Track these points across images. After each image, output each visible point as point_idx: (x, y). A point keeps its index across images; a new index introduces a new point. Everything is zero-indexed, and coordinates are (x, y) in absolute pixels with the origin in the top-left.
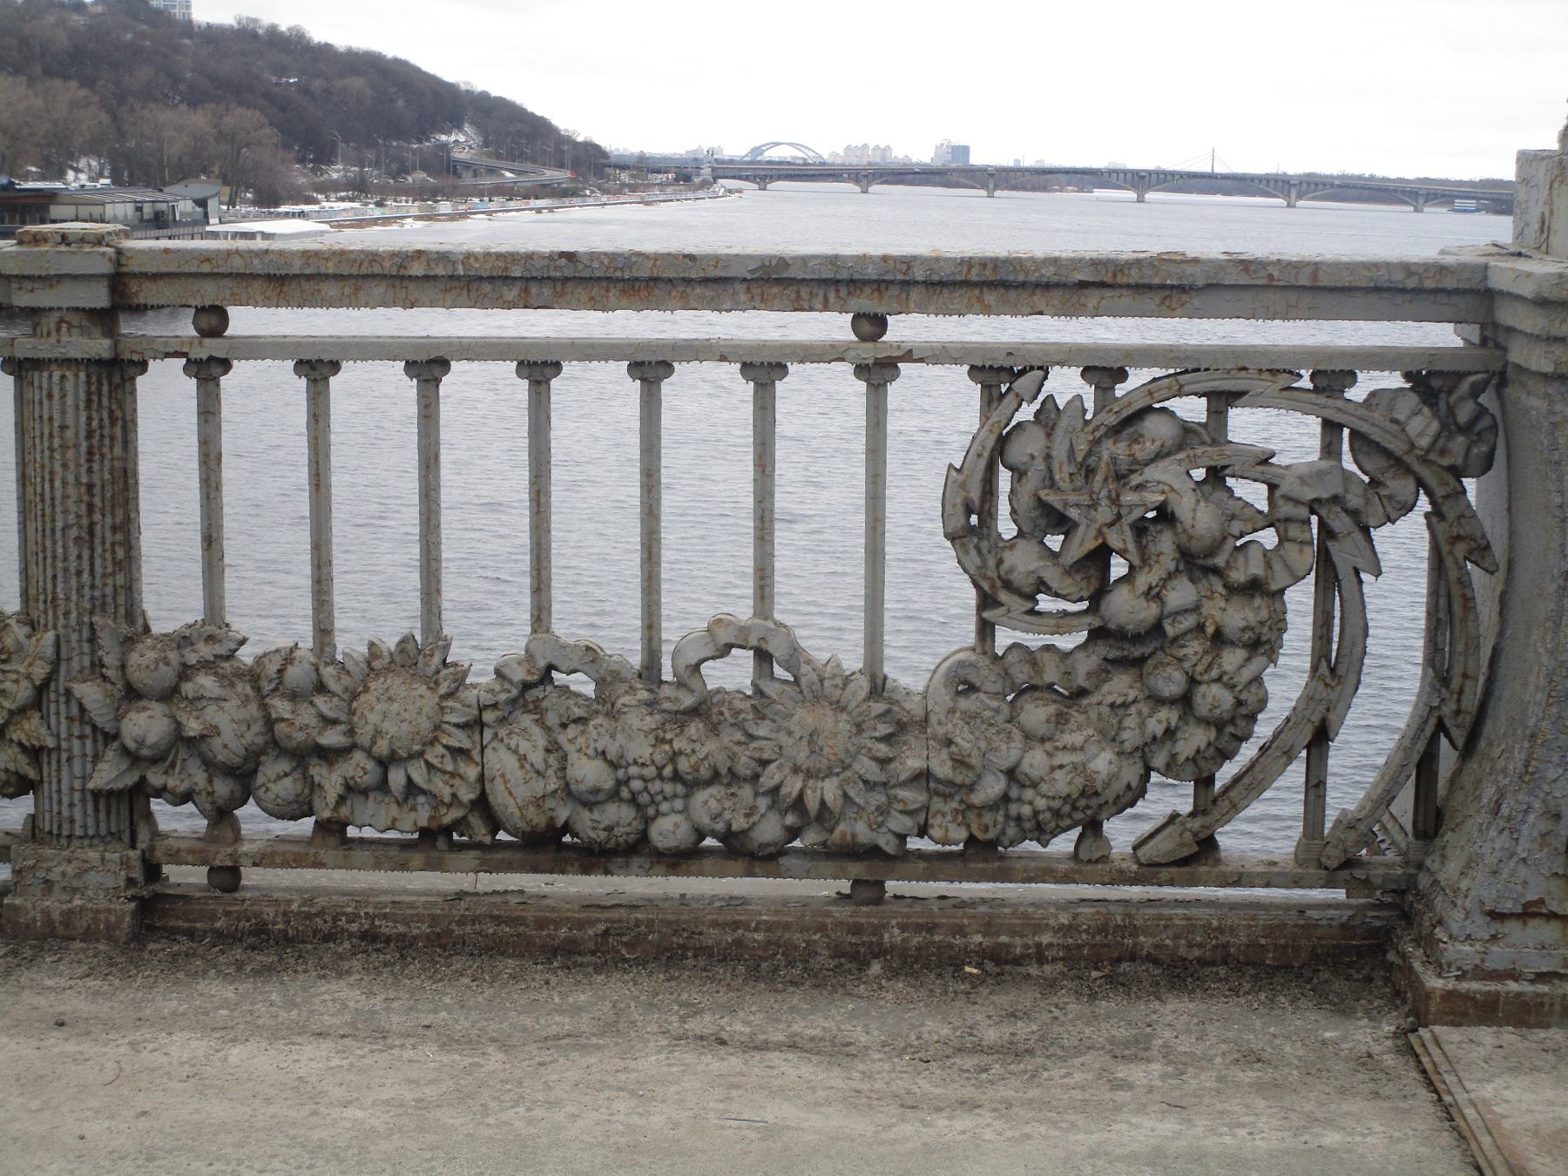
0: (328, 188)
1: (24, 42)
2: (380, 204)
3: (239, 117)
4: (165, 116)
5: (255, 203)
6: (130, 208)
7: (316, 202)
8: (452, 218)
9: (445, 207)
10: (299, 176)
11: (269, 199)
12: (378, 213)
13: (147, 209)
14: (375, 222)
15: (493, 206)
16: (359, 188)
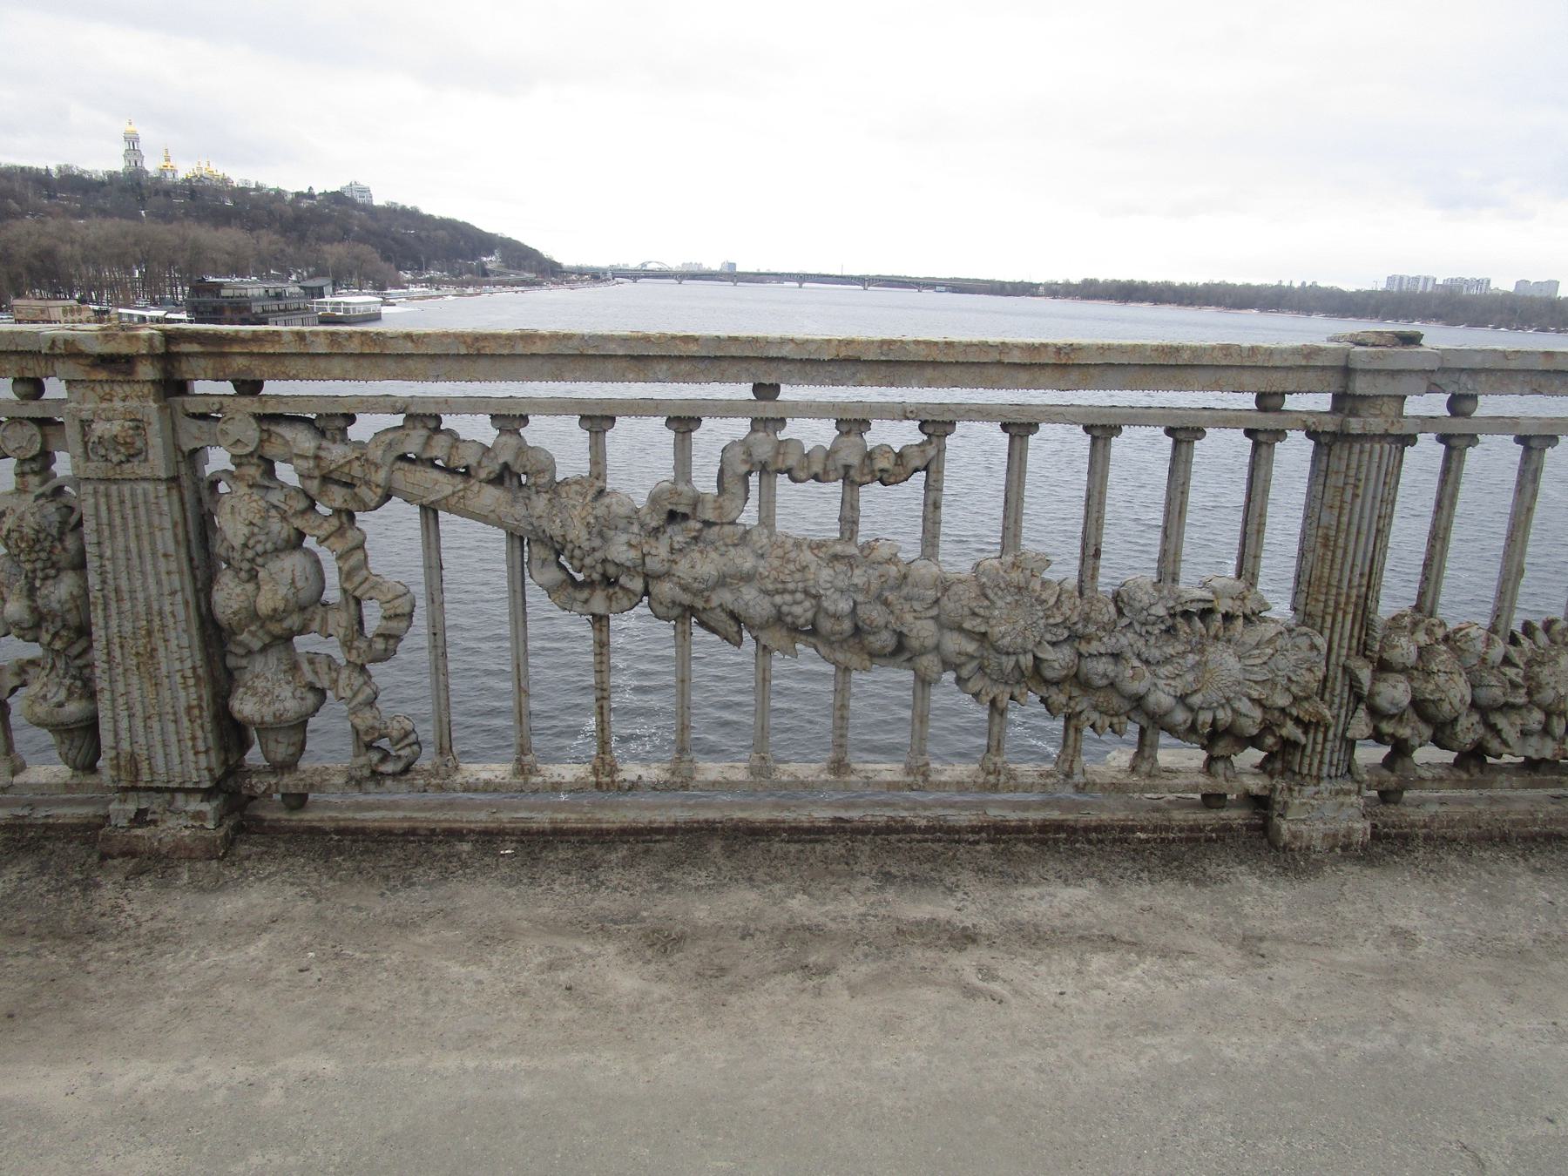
0: (414, 282)
1: (271, 213)
2: (438, 289)
3: (365, 249)
4: (327, 248)
5: (374, 288)
6: (262, 291)
7: (407, 288)
8: (471, 295)
9: (470, 290)
10: (408, 276)
11: (380, 287)
12: (434, 292)
13: (271, 292)
14: (431, 297)
15: (494, 290)
16: (431, 282)
